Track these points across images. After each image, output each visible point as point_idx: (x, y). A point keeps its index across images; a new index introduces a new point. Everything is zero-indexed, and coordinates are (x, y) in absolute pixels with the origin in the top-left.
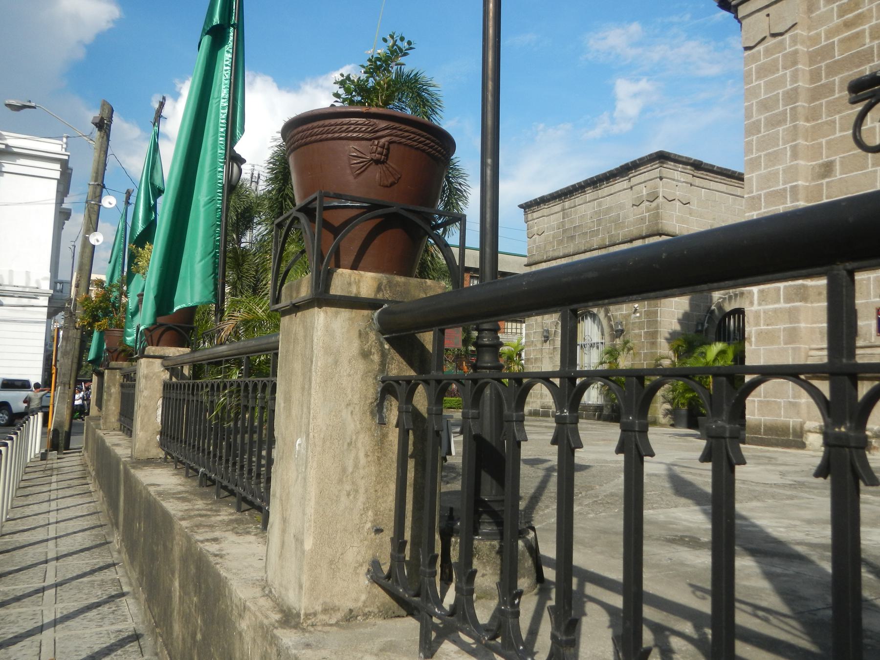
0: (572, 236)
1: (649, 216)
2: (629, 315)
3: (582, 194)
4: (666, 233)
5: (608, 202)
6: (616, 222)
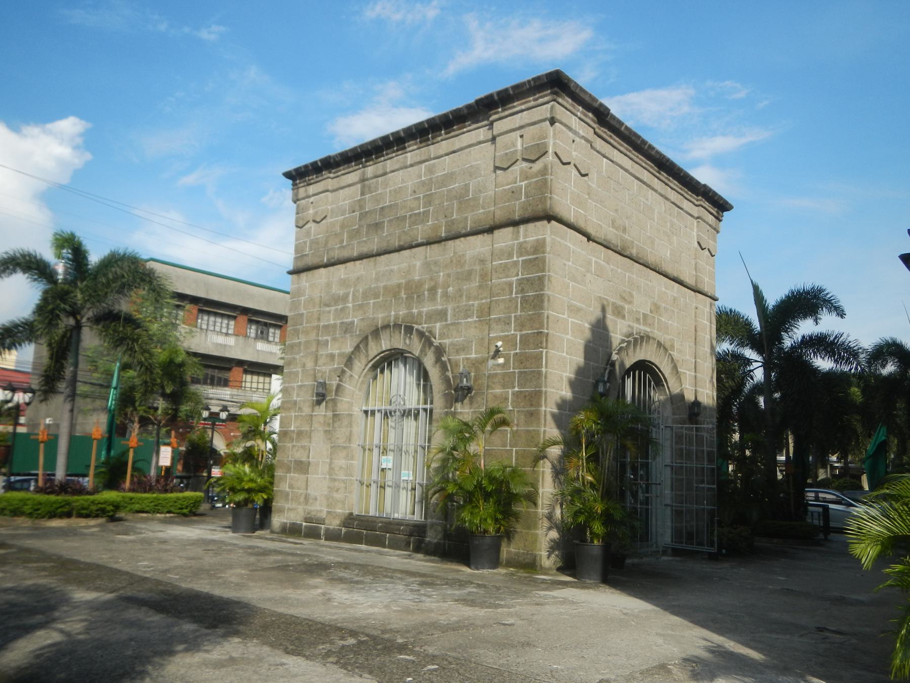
0: (377, 224)
1: (527, 187)
2: (484, 361)
3: (400, 152)
4: (559, 216)
5: (446, 165)
6: (462, 198)
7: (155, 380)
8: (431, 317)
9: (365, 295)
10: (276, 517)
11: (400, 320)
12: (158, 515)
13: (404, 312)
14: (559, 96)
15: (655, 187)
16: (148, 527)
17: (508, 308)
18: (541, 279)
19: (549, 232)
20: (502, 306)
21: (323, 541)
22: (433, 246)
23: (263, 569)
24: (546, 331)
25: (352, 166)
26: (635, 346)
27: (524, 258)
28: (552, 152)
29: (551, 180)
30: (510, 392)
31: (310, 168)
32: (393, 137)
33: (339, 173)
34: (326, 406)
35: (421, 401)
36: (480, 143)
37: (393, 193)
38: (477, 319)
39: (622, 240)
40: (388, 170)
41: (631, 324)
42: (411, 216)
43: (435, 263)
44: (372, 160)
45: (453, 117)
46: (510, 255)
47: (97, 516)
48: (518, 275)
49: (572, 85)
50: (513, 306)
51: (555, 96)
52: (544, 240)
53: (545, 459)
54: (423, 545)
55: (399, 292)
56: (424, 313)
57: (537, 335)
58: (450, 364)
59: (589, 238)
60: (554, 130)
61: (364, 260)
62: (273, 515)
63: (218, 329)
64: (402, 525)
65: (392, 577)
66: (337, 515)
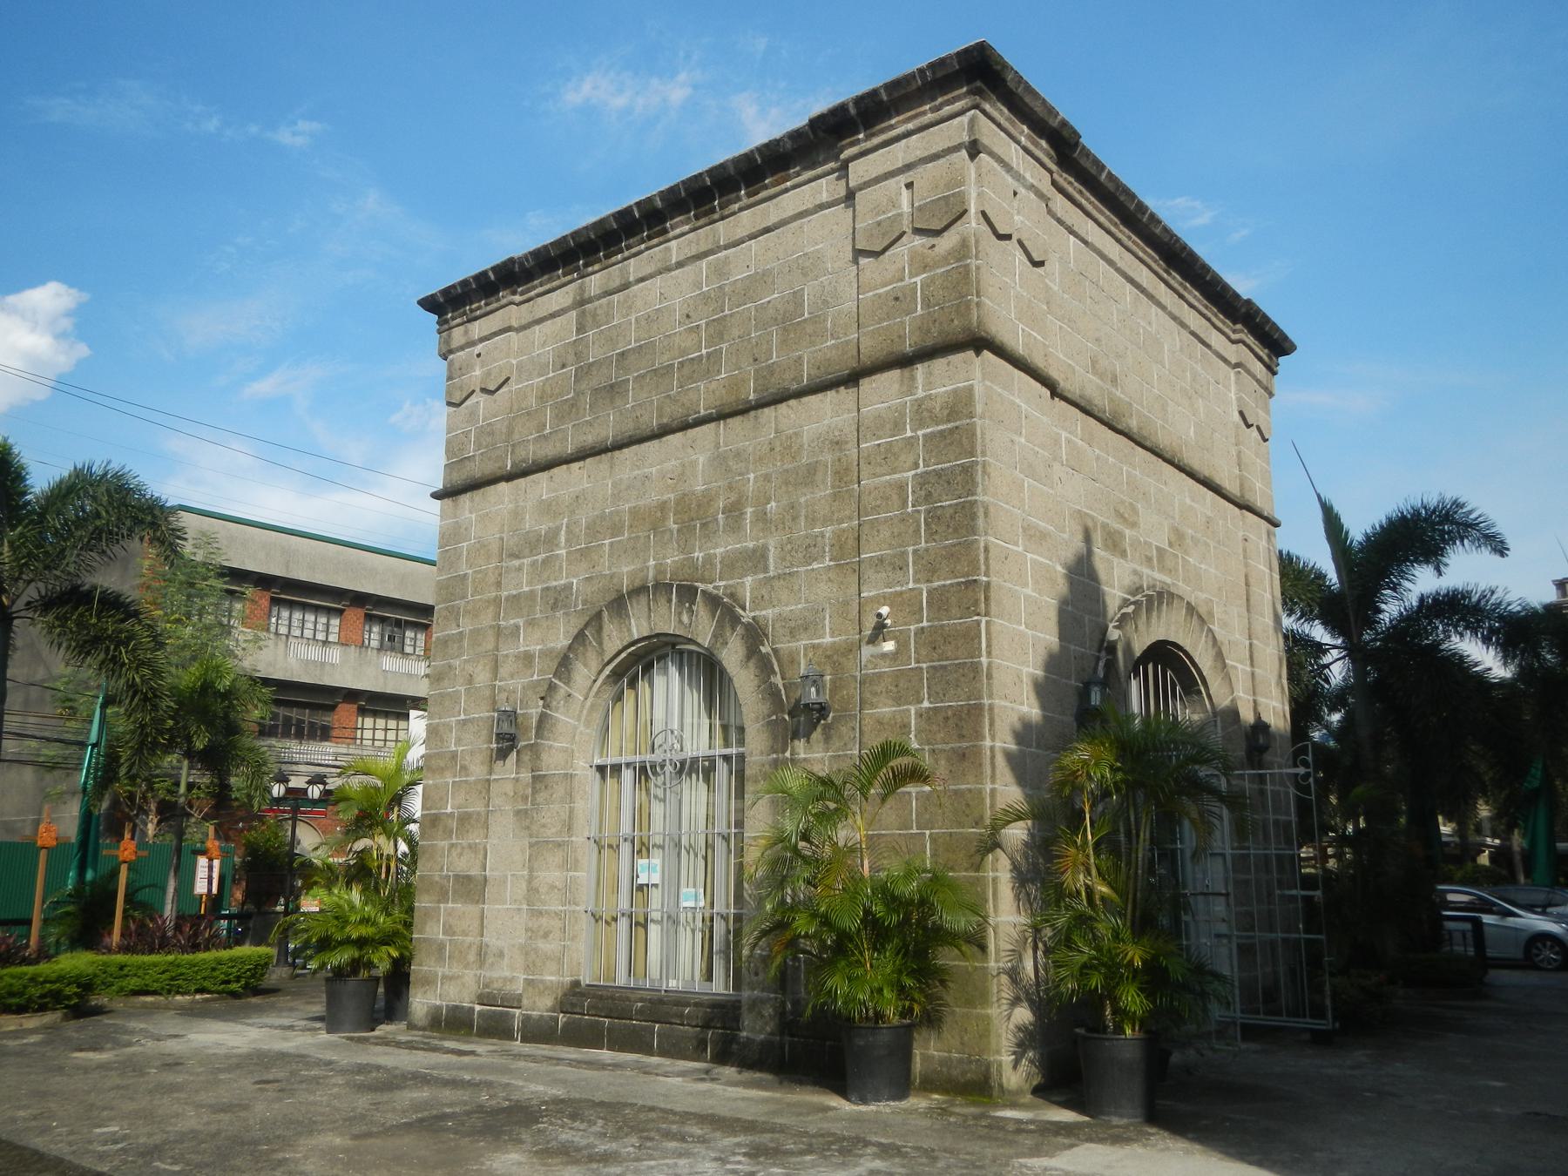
0: (612, 386)
1: (925, 285)
2: (851, 649)
3: (655, 241)
6: (790, 322)
7: (163, 721)
8: (733, 565)
9: (593, 530)
10: (419, 995)
11: (669, 576)
12: (179, 998)
13: (676, 558)
14: (985, 99)
15: (1163, 300)
16: (151, 1028)
17: (900, 534)
18: (968, 471)
19: (978, 374)
20: (885, 533)
21: (518, 1042)
22: (728, 420)
23: (389, 1131)
24: (985, 579)
25: (559, 277)
26: (1149, 610)
27: (929, 430)
28: (976, 213)
29: (978, 268)
30: (913, 712)
31: (474, 286)
32: (639, 212)
33: (533, 293)
34: (518, 761)
35: (718, 741)
36: (822, 207)
37: (643, 323)
38: (832, 563)
39: (1111, 400)
40: (631, 279)
41: (1139, 568)
42: (682, 364)
43: (738, 455)
44: (599, 261)
45: (763, 159)
46: (898, 426)
47: (42, 1008)
48: (916, 466)
49: (1010, 77)
50: (910, 531)
51: (978, 98)
52: (970, 389)
53: (998, 850)
54: (735, 1047)
55: (664, 518)
56: (718, 559)
57: (966, 588)
58: (778, 661)
59: (1055, 391)
60: (978, 168)
61: (588, 460)
62: (412, 991)
63: (308, 633)
64: (688, 1004)
65: (682, 1138)
66: (546, 988)
